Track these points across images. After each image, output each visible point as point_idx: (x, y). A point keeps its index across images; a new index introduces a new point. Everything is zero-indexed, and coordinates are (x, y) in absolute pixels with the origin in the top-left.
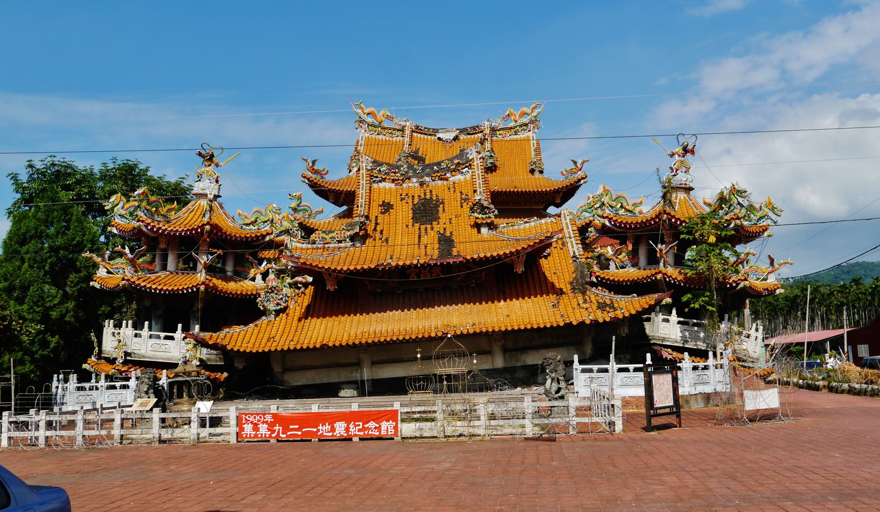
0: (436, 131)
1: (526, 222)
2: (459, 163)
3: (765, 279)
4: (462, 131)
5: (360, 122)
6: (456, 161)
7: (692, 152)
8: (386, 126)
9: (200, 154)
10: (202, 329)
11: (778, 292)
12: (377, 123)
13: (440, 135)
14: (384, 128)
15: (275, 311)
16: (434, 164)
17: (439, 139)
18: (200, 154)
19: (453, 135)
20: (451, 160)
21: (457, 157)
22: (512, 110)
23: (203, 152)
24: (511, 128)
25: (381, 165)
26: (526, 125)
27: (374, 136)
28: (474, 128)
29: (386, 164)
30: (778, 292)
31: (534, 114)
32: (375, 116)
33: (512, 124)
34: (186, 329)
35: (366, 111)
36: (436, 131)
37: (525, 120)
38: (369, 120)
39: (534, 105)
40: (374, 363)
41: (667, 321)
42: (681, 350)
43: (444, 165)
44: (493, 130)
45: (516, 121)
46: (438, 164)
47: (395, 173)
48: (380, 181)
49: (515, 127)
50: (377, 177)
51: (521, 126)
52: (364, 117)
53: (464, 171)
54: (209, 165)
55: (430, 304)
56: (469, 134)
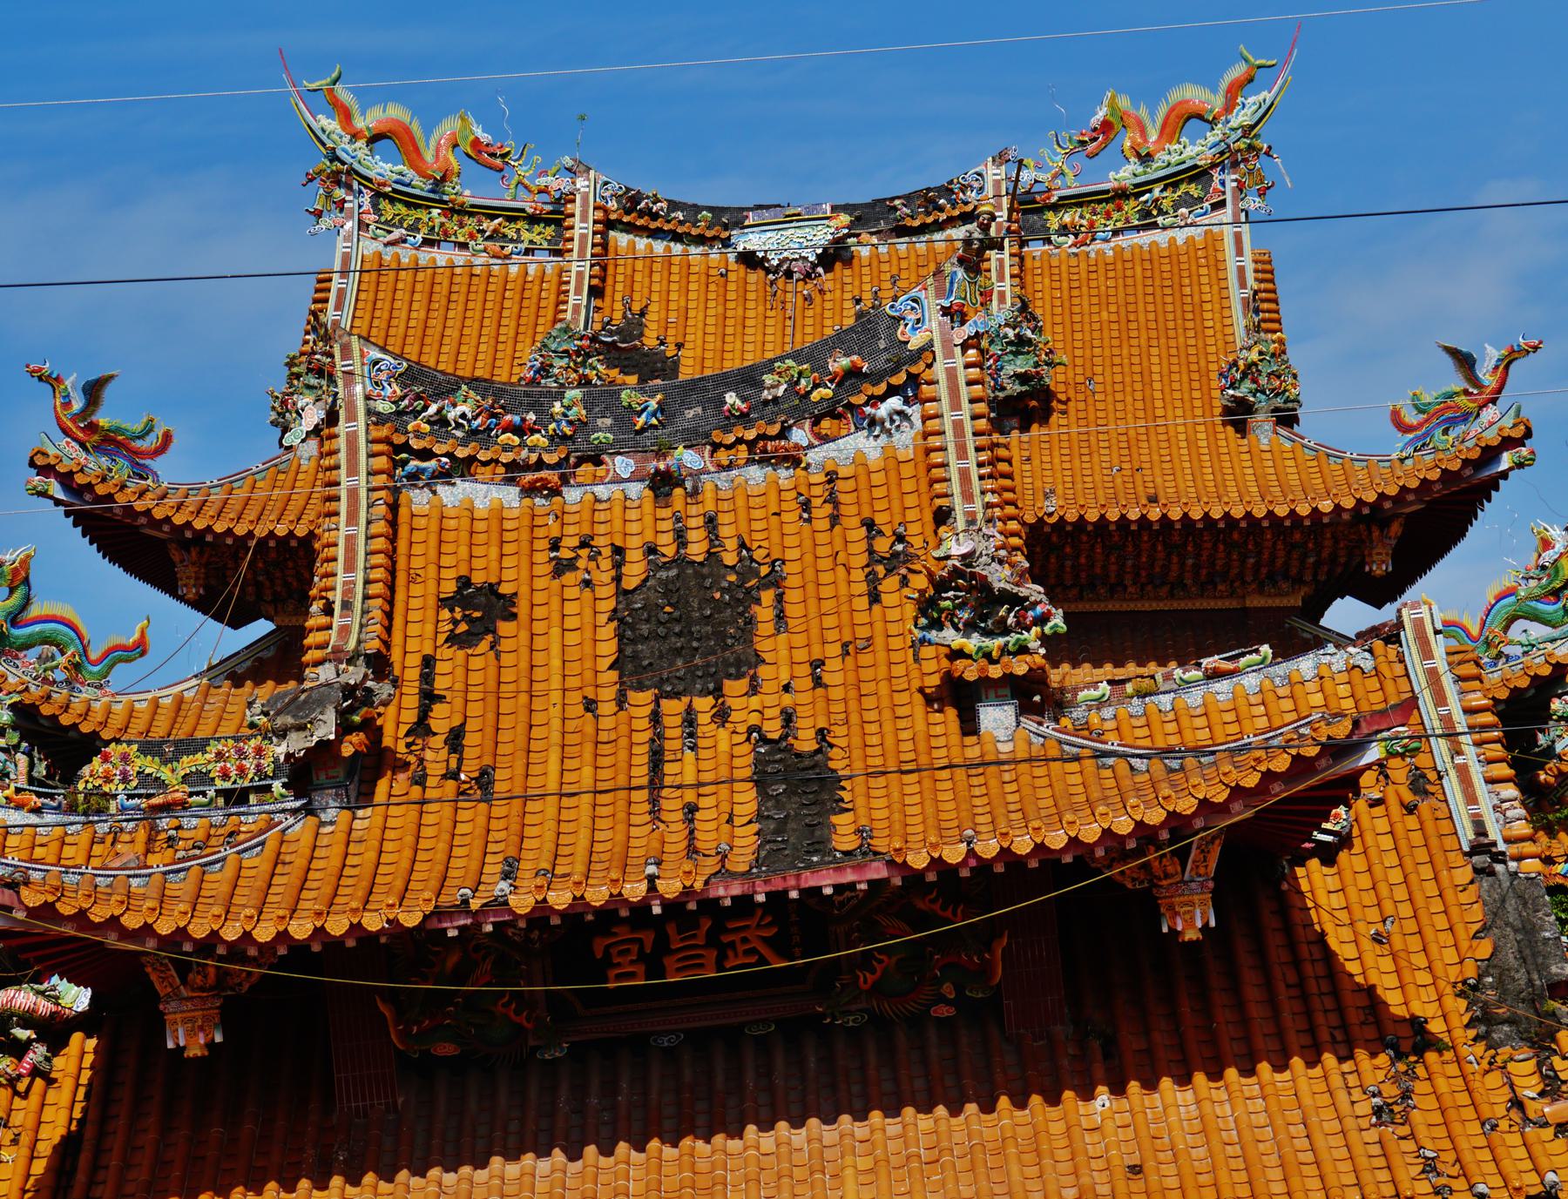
1: (1215, 675)
2: (853, 373)
4: (865, 216)
5: (336, 179)
8: (468, 197)
12: (420, 186)
13: (752, 241)
14: (457, 211)
16: (726, 381)
17: (749, 260)
19: (821, 235)
20: (814, 356)
21: (841, 341)
22: (1124, 103)
24: (1121, 195)
25: (446, 388)
26: (1199, 175)
28: (927, 199)
29: (474, 382)
31: (1242, 117)
33: (1126, 174)
36: (734, 218)
37: (1195, 149)
38: (382, 168)
39: (1238, 71)
43: (774, 386)
44: (1030, 207)
45: (1146, 159)
46: (748, 379)
47: (519, 430)
48: (445, 476)
50: (426, 454)
51: (1171, 181)
52: (356, 153)
53: (883, 410)
56: (902, 231)
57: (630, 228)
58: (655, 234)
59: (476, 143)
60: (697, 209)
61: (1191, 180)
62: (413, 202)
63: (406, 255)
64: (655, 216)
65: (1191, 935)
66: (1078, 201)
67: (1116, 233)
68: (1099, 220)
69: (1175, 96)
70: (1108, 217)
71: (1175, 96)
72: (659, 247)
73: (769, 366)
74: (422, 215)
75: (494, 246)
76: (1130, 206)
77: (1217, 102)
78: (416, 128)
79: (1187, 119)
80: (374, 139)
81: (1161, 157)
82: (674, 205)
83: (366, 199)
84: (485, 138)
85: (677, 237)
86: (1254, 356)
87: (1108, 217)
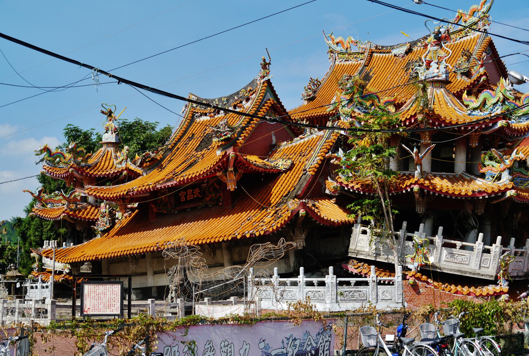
0: (392, 47)
1: (301, 138)
2: (250, 91)
3: (499, 178)
4: (414, 44)
5: (332, 52)
6: (249, 89)
9: (103, 112)
10: (74, 245)
11: (508, 194)
12: (344, 51)
13: (394, 52)
14: (350, 54)
15: (101, 231)
17: (395, 56)
18: (103, 112)
20: (245, 88)
21: (249, 85)
23: (104, 110)
24: (461, 30)
26: (476, 23)
27: (342, 63)
30: (508, 194)
31: (484, 9)
32: (343, 44)
34: (505, 243)
35: (337, 40)
36: (392, 47)
37: (474, 19)
38: (339, 49)
40: (155, 273)
41: (364, 232)
43: (241, 94)
46: (237, 93)
48: (201, 115)
50: (197, 113)
52: (334, 47)
54: (110, 120)
55: (177, 223)
57: (377, 52)
58: (381, 53)
59: (352, 42)
60: (388, 47)
61: (475, 25)
62: (343, 54)
63: (342, 63)
64: (380, 49)
65: (232, 190)
67: (460, 38)
68: (458, 36)
69: (472, 8)
70: (459, 35)
71: (472, 8)
72: (381, 55)
73: (240, 91)
74: (344, 56)
75: (356, 59)
76: (463, 32)
77: (480, 7)
78: (344, 41)
80: (337, 43)
81: (468, 21)
82: (383, 47)
83: (336, 55)
84: (353, 40)
85: (384, 53)
86: (460, 62)
87: (459, 35)
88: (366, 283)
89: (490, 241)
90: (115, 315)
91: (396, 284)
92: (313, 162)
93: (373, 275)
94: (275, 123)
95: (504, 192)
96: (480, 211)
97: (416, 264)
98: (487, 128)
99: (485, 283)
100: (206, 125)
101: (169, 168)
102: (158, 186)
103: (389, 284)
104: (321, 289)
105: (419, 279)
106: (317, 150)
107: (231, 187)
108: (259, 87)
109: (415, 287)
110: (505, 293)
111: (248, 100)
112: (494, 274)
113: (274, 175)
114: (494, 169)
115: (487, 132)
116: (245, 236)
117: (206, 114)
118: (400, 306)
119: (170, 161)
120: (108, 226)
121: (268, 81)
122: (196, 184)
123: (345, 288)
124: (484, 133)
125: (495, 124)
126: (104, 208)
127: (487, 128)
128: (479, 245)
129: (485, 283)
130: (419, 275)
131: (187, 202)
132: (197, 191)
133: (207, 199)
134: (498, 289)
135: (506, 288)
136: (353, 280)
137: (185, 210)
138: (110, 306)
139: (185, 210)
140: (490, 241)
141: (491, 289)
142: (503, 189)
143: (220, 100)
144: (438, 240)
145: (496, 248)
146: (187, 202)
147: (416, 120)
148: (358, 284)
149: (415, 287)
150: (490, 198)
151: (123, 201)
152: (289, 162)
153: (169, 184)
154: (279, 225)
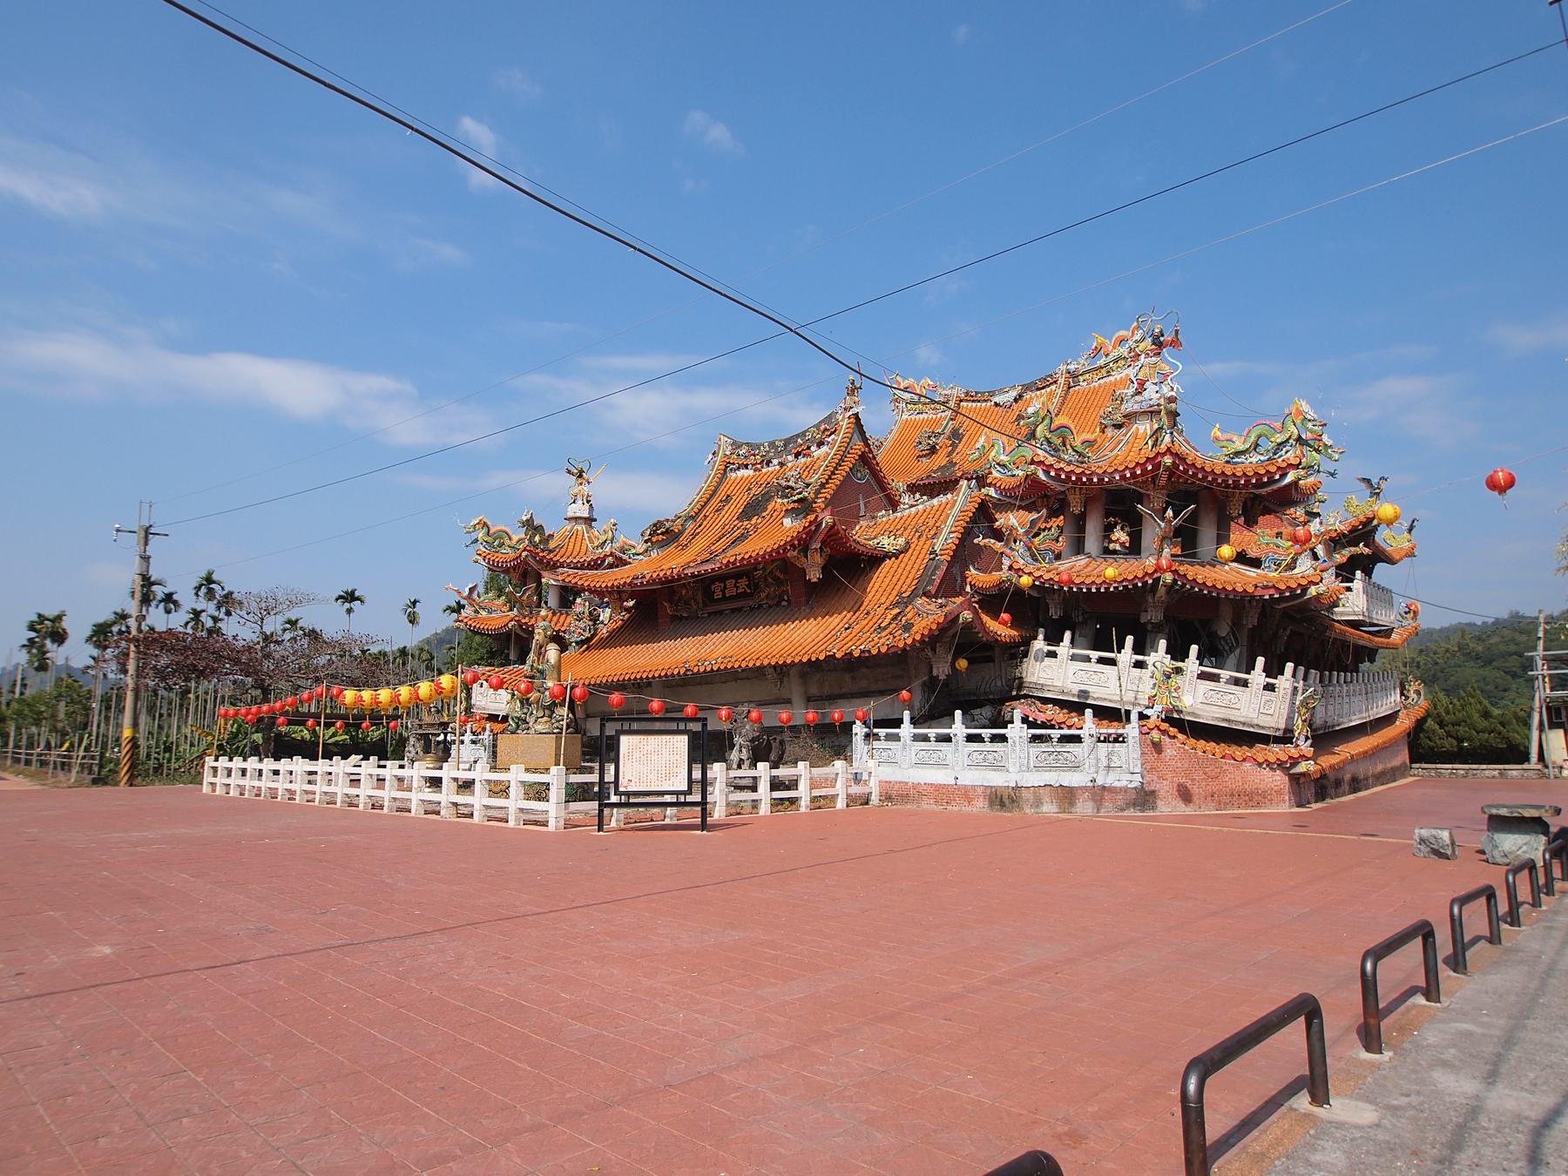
3: (1291, 566)
7: (1175, 343)
13: (997, 399)
16: (798, 436)
17: (996, 404)
19: (1014, 394)
20: (817, 426)
25: (740, 446)
30: (1313, 591)
33: (1102, 362)
36: (992, 394)
42: (1077, 707)
44: (1074, 375)
46: (804, 434)
49: (1106, 365)
51: (1116, 361)
66: (1088, 372)
79: (1122, 341)
88: (1077, 739)
89: (1273, 670)
90: (677, 793)
91: (1130, 740)
92: (946, 540)
93: (1089, 725)
94: (865, 478)
95: (1305, 589)
96: (1251, 620)
97: (1158, 708)
98: (1272, 481)
99: (1265, 739)
100: (748, 485)
101: (699, 544)
102: (688, 571)
103: (1116, 741)
104: (998, 747)
105: (1164, 732)
106: (950, 521)
107: (814, 575)
108: (845, 424)
109: (1157, 747)
110: (1304, 757)
111: (820, 444)
112: (1282, 726)
113: (876, 559)
114: (1281, 551)
115: (1263, 491)
116: (851, 654)
117: (746, 467)
118: (1138, 778)
119: (694, 535)
120: (587, 635)
121: (856, 415)
122: (746, 572)
123: (1044, 747)
124: (1257, 492)
125: (1283, 476)
126: (581, 605)
127: (1272, 481)
128: (1258, 677)
129: (1265, 739)
130: (1165, 726)
131: (724, 599)
132: (743, 582)
133: (763, 595)
134: (1294, 752)
135: (1309, 751)
136: (1056, 733)
137: (721, 612)
138: (668, 777)
139: (721, 612)
140: (1273, 670)
141: (1277, 751)
142: (1304, 582)
143: (772, 444)
144: (1192, 664)
145: (1284, 682)
146: (724, 599)
147: (1157, 466)
148: (1066, 739)
149: (1157, 747)
150: (1282, 599)
151: (616, 595)
152: (901, 541)
153: (709, 567)
154: (909, 641)
